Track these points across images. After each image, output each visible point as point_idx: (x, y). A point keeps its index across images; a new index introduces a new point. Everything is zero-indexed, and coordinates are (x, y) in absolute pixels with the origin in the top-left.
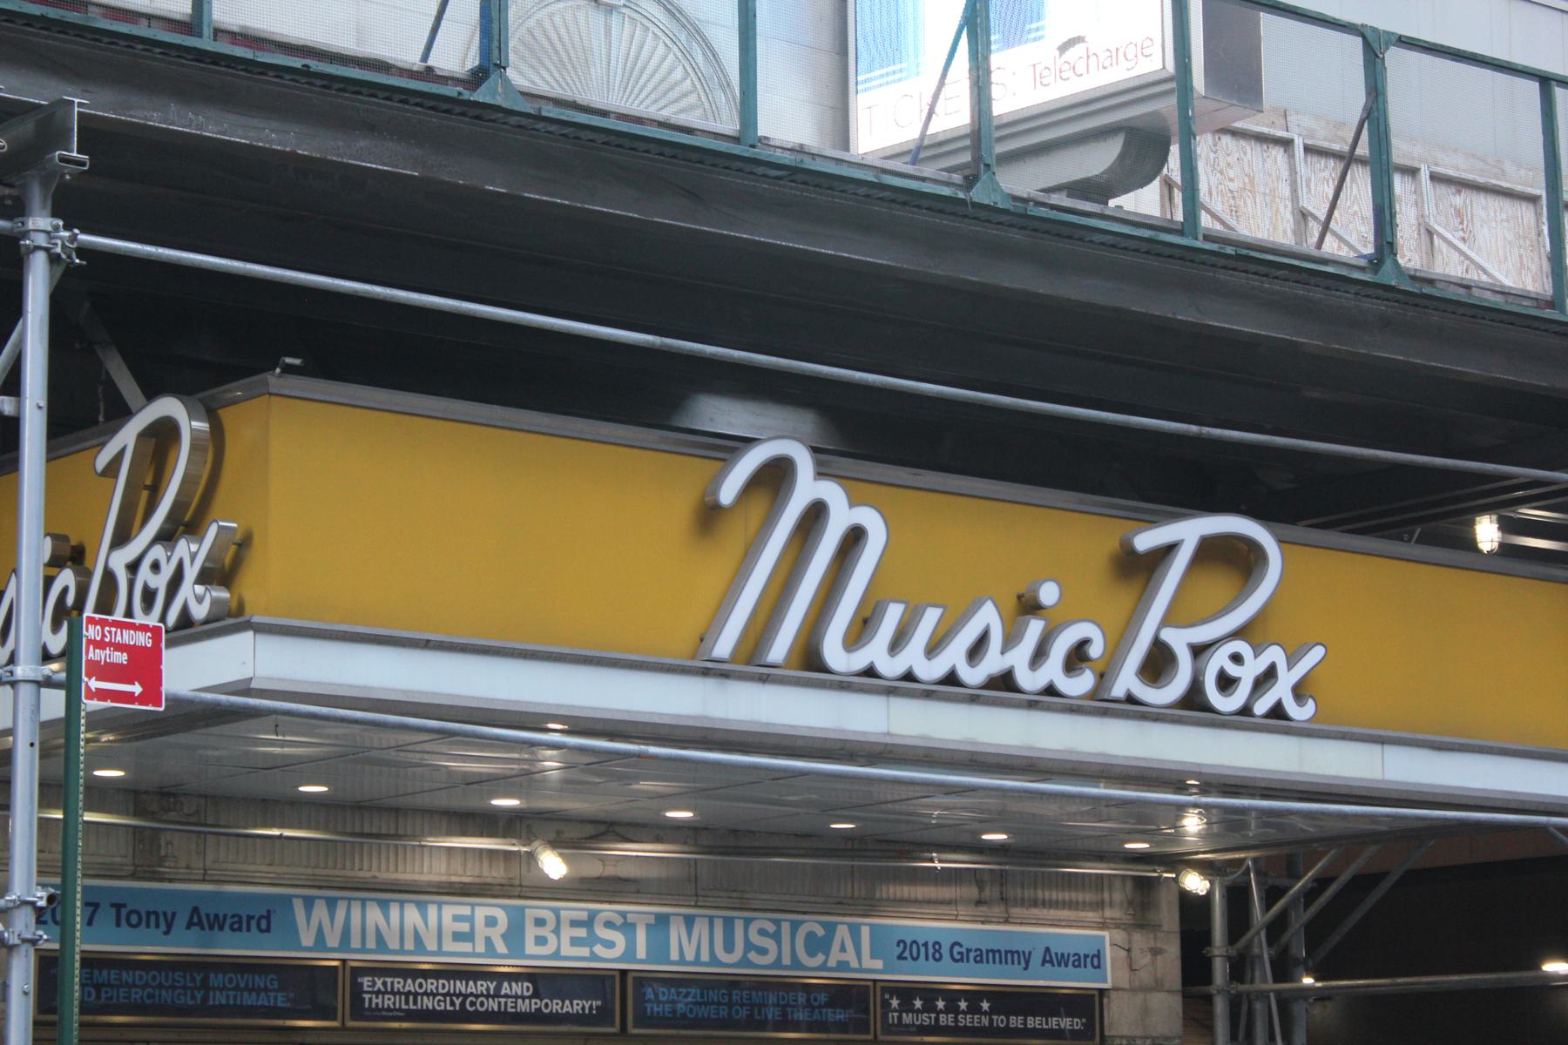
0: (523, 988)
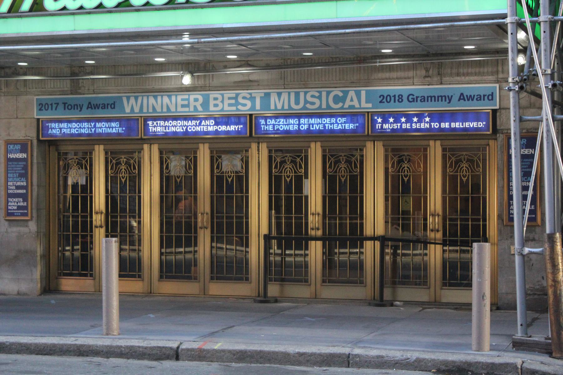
0: (212, 122)
